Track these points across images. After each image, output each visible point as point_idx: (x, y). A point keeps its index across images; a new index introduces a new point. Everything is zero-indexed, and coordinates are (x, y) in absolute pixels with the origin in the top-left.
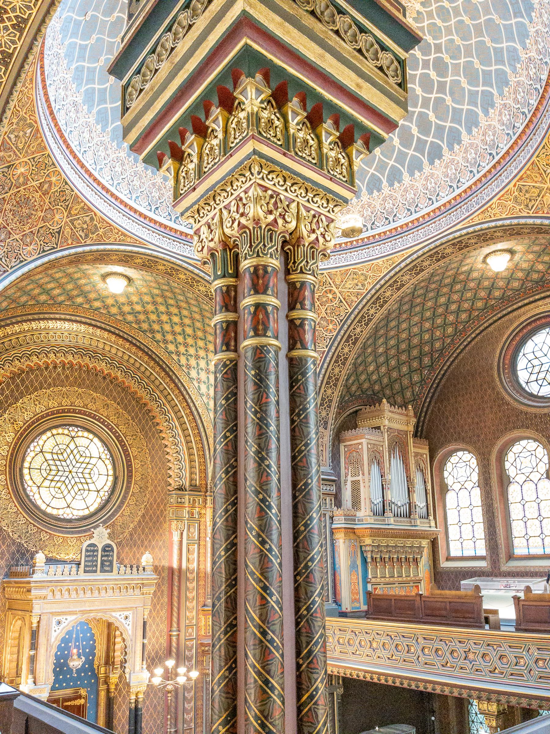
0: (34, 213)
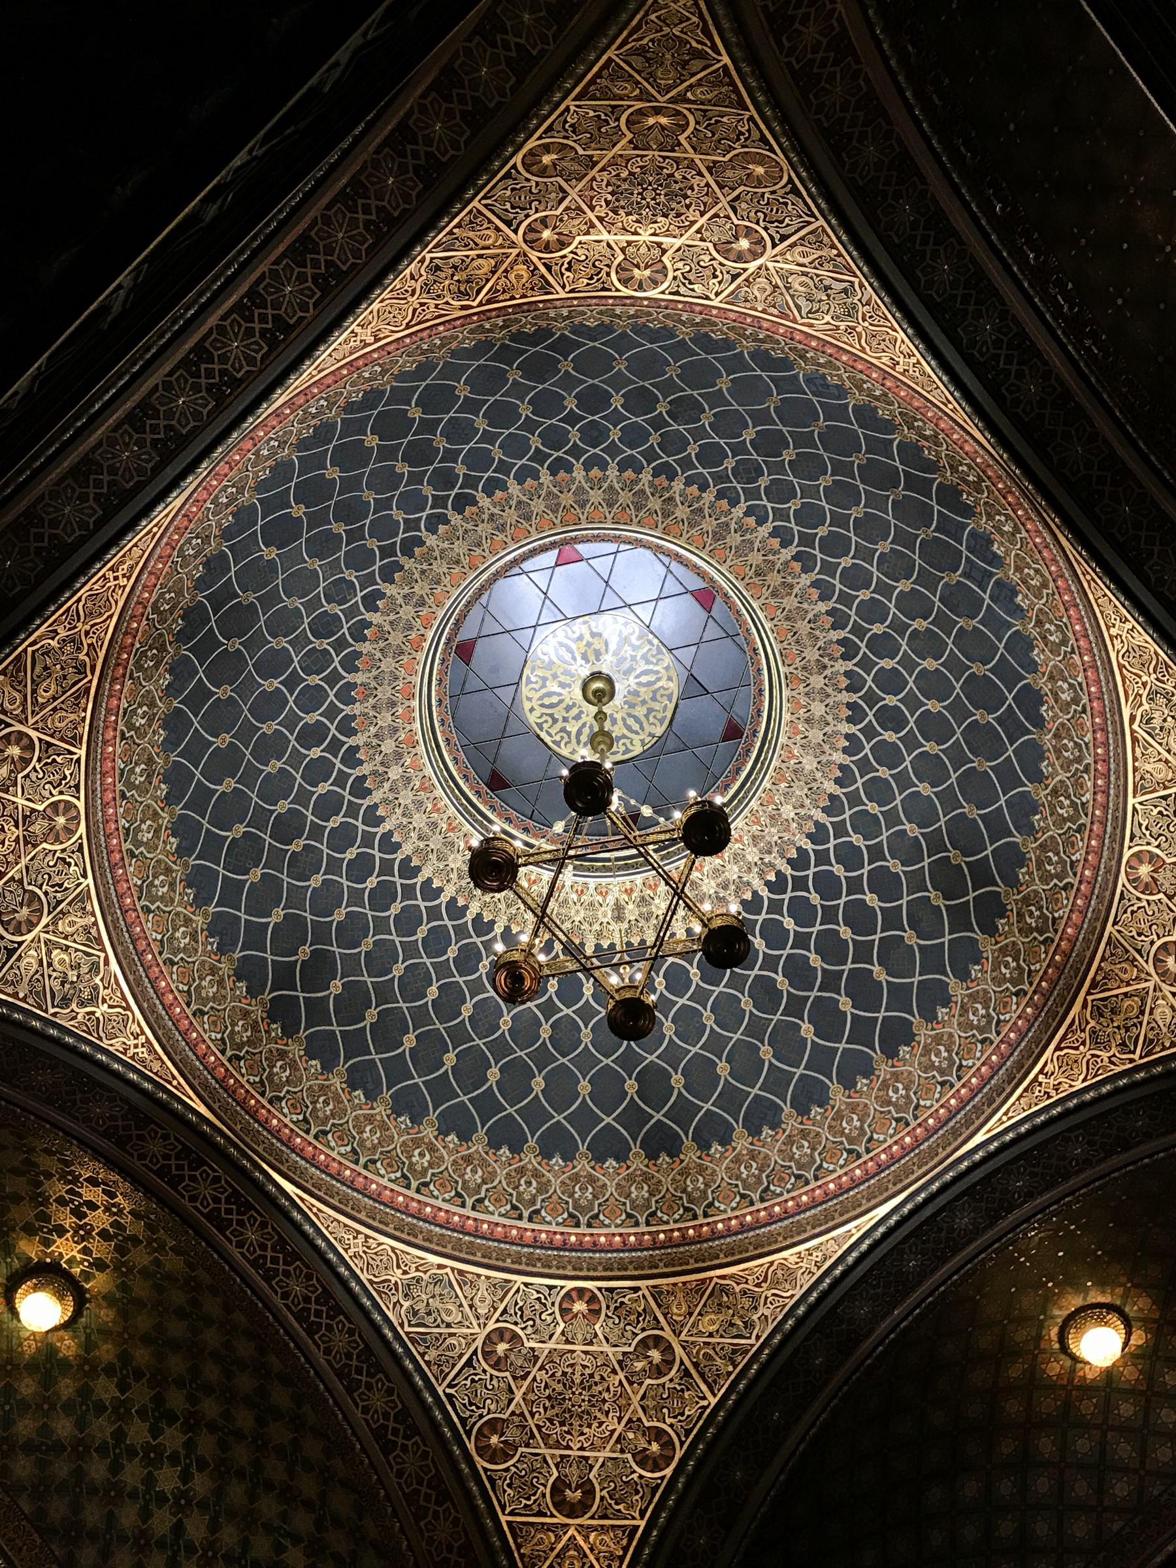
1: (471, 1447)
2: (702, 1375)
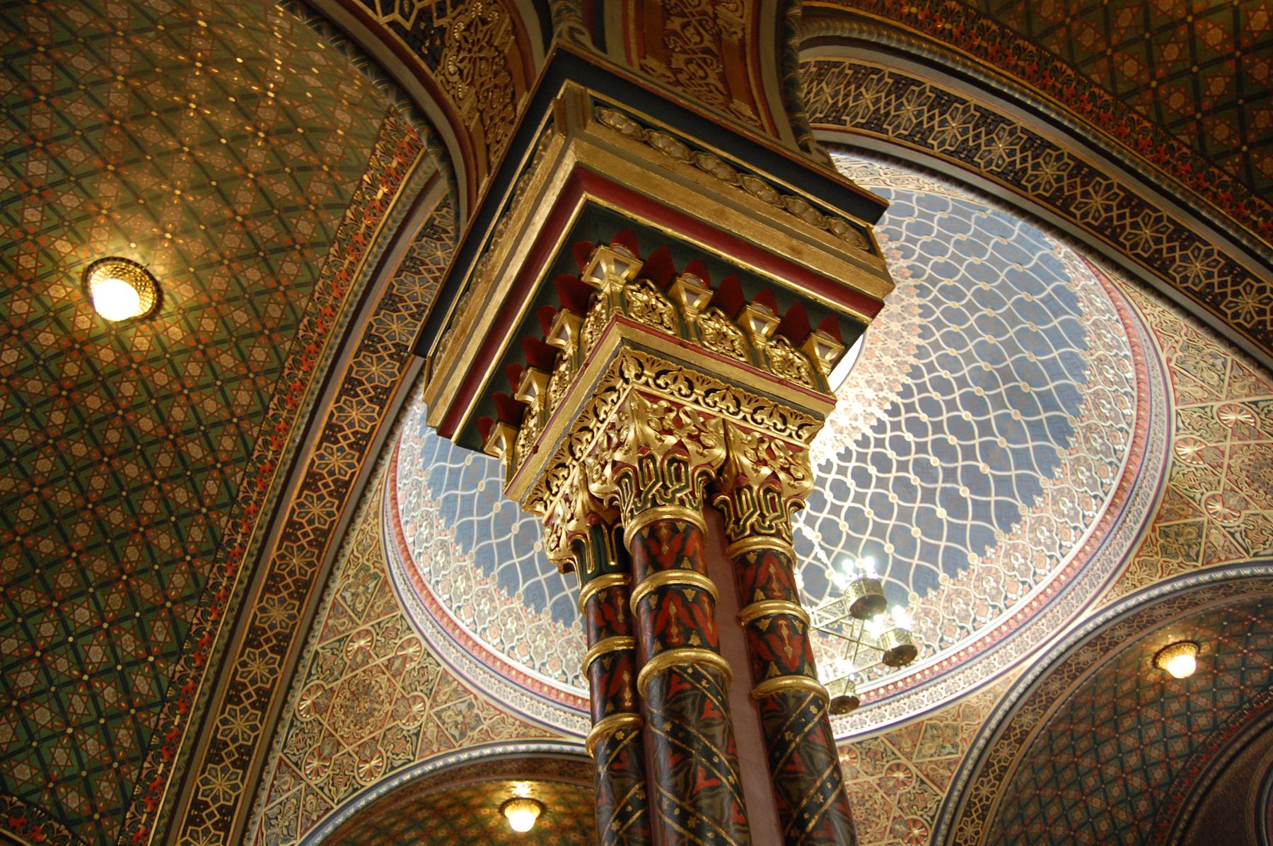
0: (377, 706)
2: (933, 781)
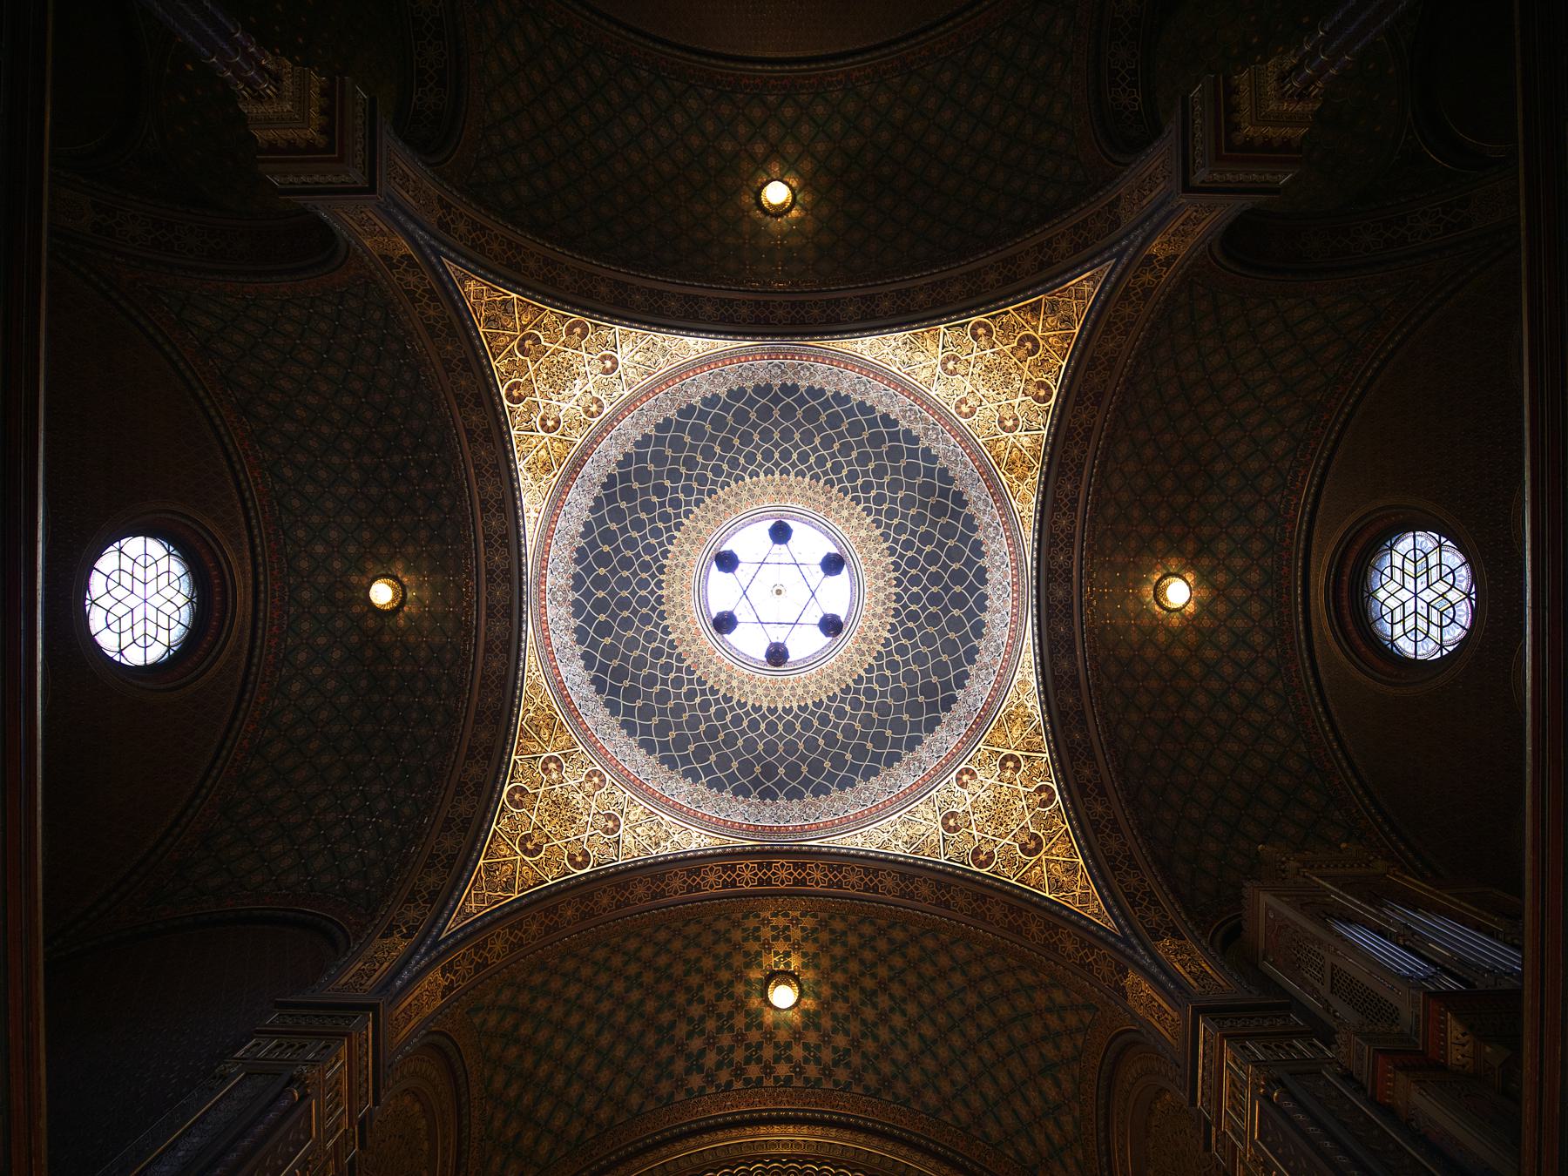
1: (975, 869)
